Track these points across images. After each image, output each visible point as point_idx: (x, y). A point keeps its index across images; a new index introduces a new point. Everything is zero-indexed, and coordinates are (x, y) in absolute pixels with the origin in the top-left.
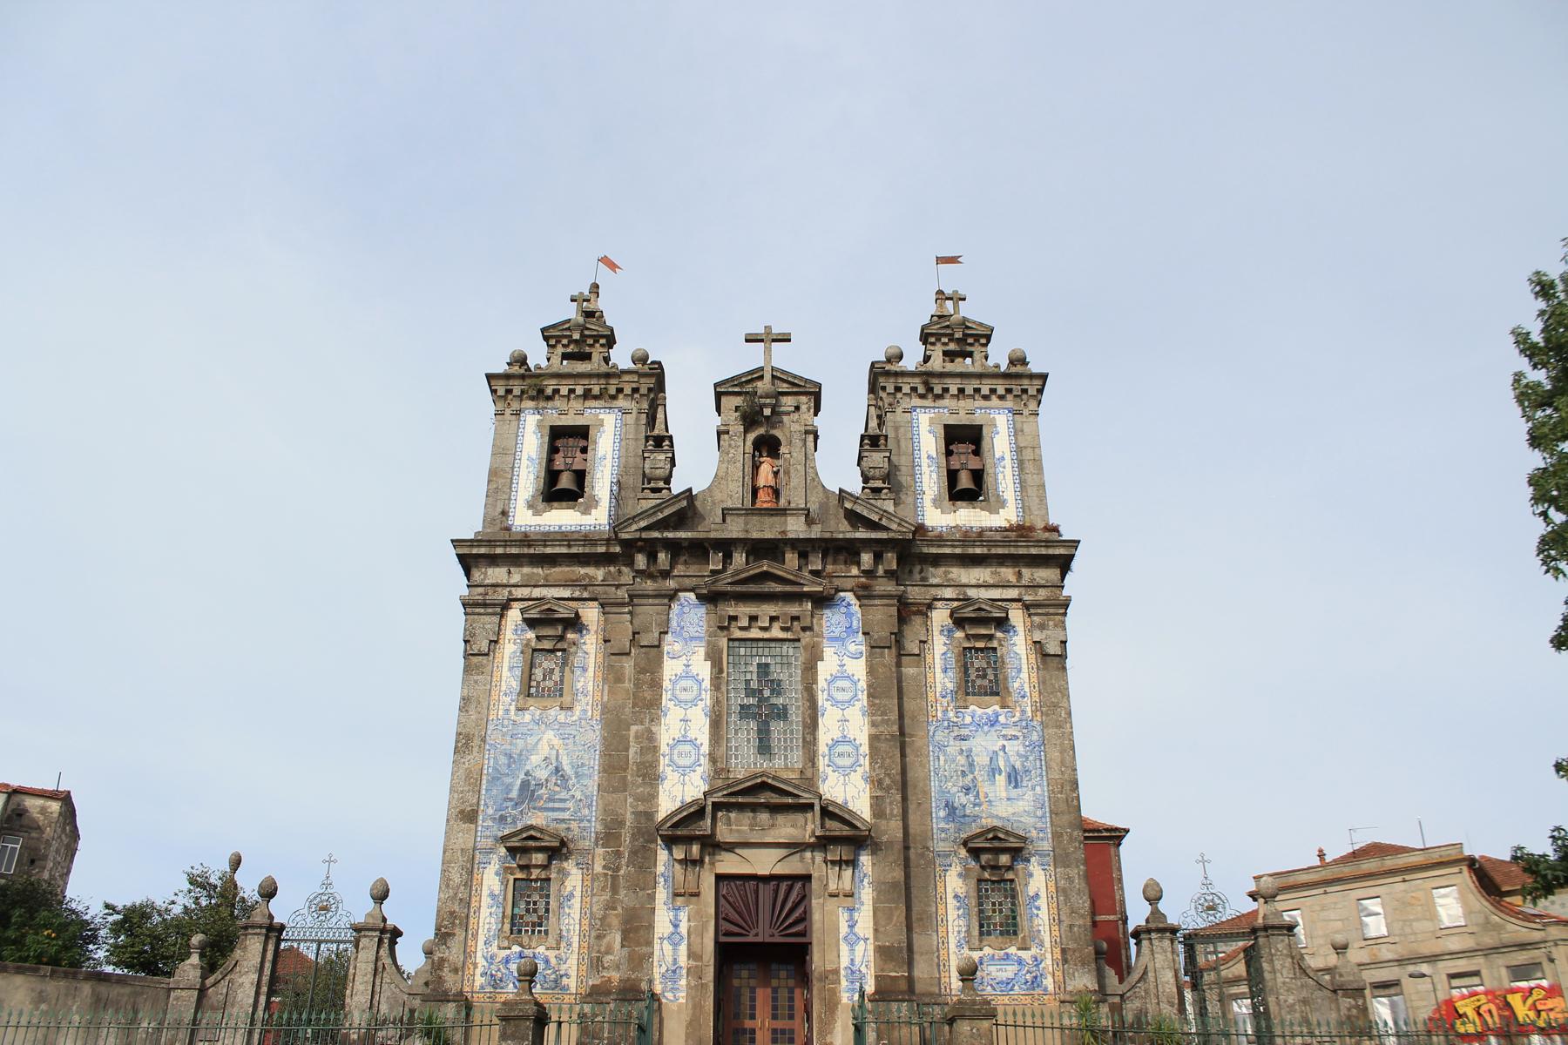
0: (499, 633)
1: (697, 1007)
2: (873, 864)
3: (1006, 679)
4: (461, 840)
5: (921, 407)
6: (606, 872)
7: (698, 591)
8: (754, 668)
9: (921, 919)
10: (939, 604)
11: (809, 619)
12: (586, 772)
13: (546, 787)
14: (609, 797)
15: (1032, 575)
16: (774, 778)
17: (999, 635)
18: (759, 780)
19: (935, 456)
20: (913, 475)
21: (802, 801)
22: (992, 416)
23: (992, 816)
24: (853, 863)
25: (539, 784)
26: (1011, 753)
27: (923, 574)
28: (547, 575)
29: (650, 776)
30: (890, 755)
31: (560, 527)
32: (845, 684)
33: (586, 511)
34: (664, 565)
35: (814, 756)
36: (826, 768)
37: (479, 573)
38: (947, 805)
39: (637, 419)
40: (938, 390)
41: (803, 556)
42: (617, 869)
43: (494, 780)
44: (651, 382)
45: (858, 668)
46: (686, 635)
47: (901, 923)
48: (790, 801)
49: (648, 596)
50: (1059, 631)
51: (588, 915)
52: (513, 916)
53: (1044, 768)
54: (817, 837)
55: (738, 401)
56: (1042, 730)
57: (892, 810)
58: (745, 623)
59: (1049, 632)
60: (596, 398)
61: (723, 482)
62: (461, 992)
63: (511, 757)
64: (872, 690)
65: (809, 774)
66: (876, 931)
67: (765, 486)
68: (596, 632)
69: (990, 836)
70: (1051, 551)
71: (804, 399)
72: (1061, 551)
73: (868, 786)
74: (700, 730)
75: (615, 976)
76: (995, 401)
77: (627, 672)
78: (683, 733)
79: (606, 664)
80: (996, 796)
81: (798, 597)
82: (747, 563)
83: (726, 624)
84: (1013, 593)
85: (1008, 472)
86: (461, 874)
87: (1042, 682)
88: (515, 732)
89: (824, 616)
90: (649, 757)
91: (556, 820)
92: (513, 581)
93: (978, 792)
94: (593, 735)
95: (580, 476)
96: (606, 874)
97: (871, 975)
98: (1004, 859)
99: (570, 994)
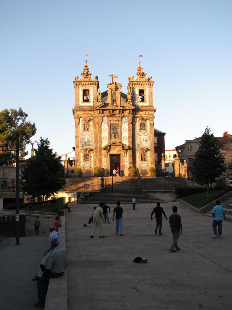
3: (146, 128)
14: (96, 144)
29: (101, 141)
32: (125, 129)
33: (89, 103)
40: (138, 84)
42: (97, 153)
44: (97, 83)
45: (127, 127)
55: (110, 87)
74: (107, 135)
75: (98, 166)
76: (146, 86)
82: (113, 112)
84: (147, 116)
90: (101, 139)
94: (93, 136)
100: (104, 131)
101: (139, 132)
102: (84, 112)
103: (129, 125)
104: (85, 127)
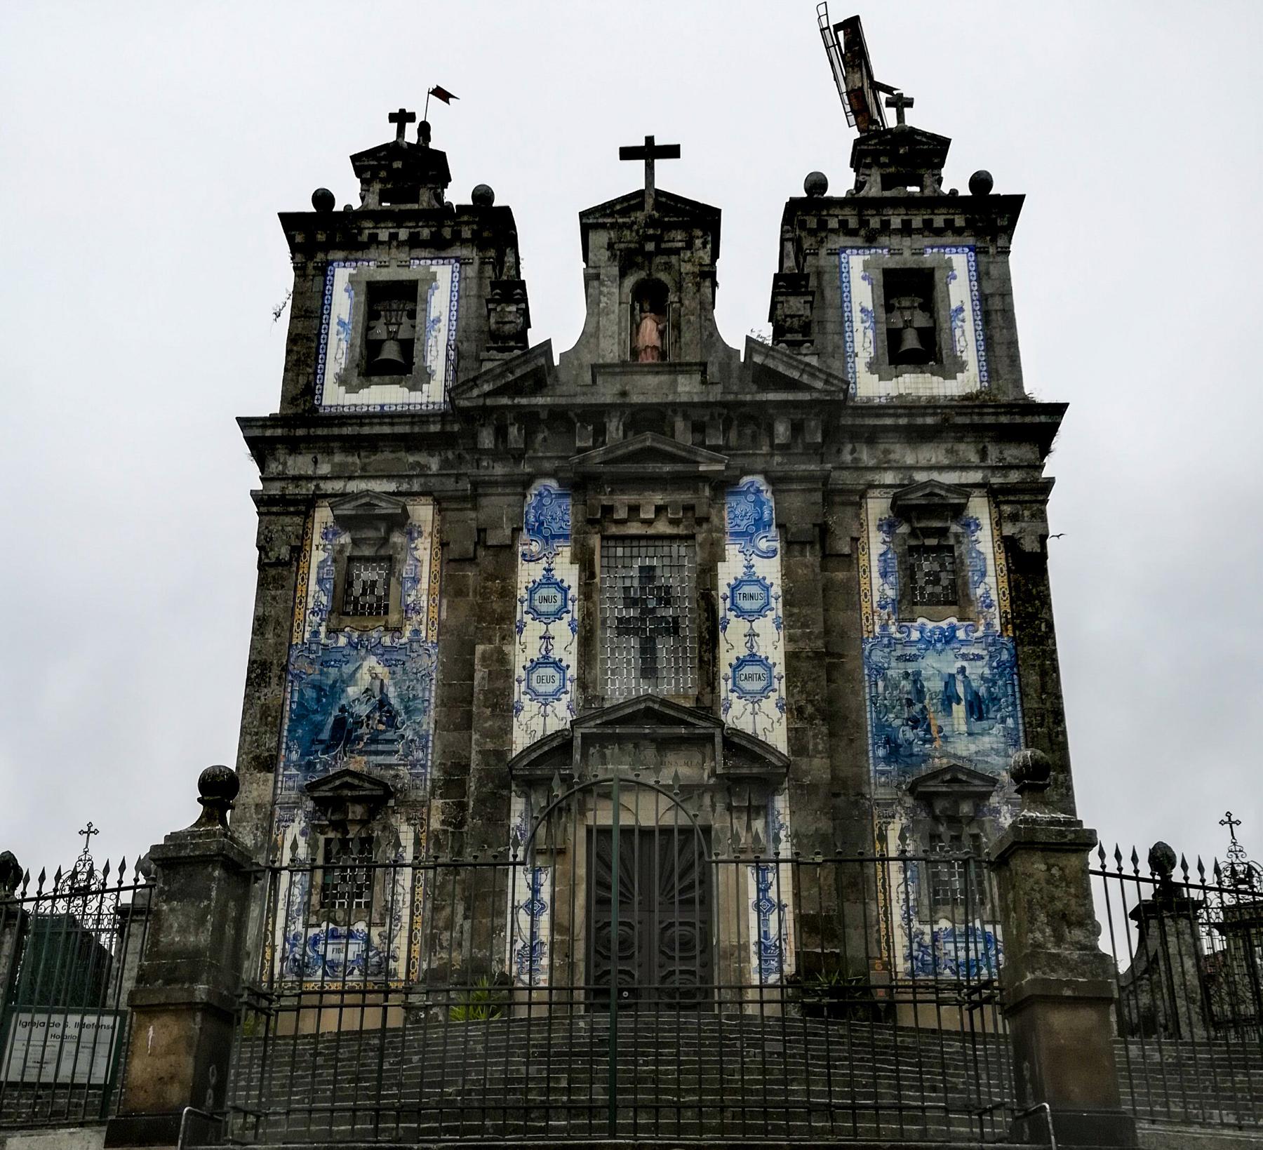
0: (303, 538)
2: (792, 813)
3: (966, 584)
4: (255, 794)
5: (852, 248)
6: (445, 828)
7: (561, 475)
8: (635, 573)
9: (855, 884)
10: (876, 492)
11: (705, 508)
12: (420, 706)
13: (368, 725)
14: (452, 736)
15: (1001, 453)
16: (664, 702)
17: (955, 528)
18: (642, 706)
19: (870, 308)
20: (842, 333)
21: (697, 731)
22: (947, 256)
24: (762, 809)
25: (358, 723)
26: (973, 677)
27: (855, 455)
28: (365, 464)
29: (504, 708)
30: (813, 676)
31: (382, 406)
33: (415, 387)
34: (516, 442)
35: (714, 679)
36: (730, 694)
37: (276, 464)
38: (888, 741)
39: (481, 272)
40: (875, 223)
41: (698, 428)
43: (302, 714)
45: (771, 570)
46: (546, 533)
47: (830, 886)
48: (683, 731)
49: (495, 484)
50: (1036, 524)
51: (422, 882)
52: (325, 887)
53: (1018, 695)
54: (718, 776)
56: (1015, 648)
57: (816, 745)
58: (622, 514)
59: (1023, 525)
60: (424, 245)
61: (592, 340)
64: (789, 597)
65: (707, 701)
66: (797, 895)
67: (647, 347)
68: (431, 534)
69: (948, 777)
73: (784, 715)
76: (949, 239)
77: (471, 582)
78: (544, 653)
79: (444, 574)
80: (953, 731)
81: (692, 480)
83: (599, 516)
84: (975, 477)
85: (969, 326)
86: (255, 835)
87: (1014, 587)
88: (326, 658)
89: (726, 506)
90: (499, 684)
91: (380, 765)
93: (929, 725)
95: (407, 347)
96: (445, 832)
97: (791, 952)
98: (966, 808)
99: (397, 981)
100: (538, 615)
101: (893, 629)
104: (357, 589)
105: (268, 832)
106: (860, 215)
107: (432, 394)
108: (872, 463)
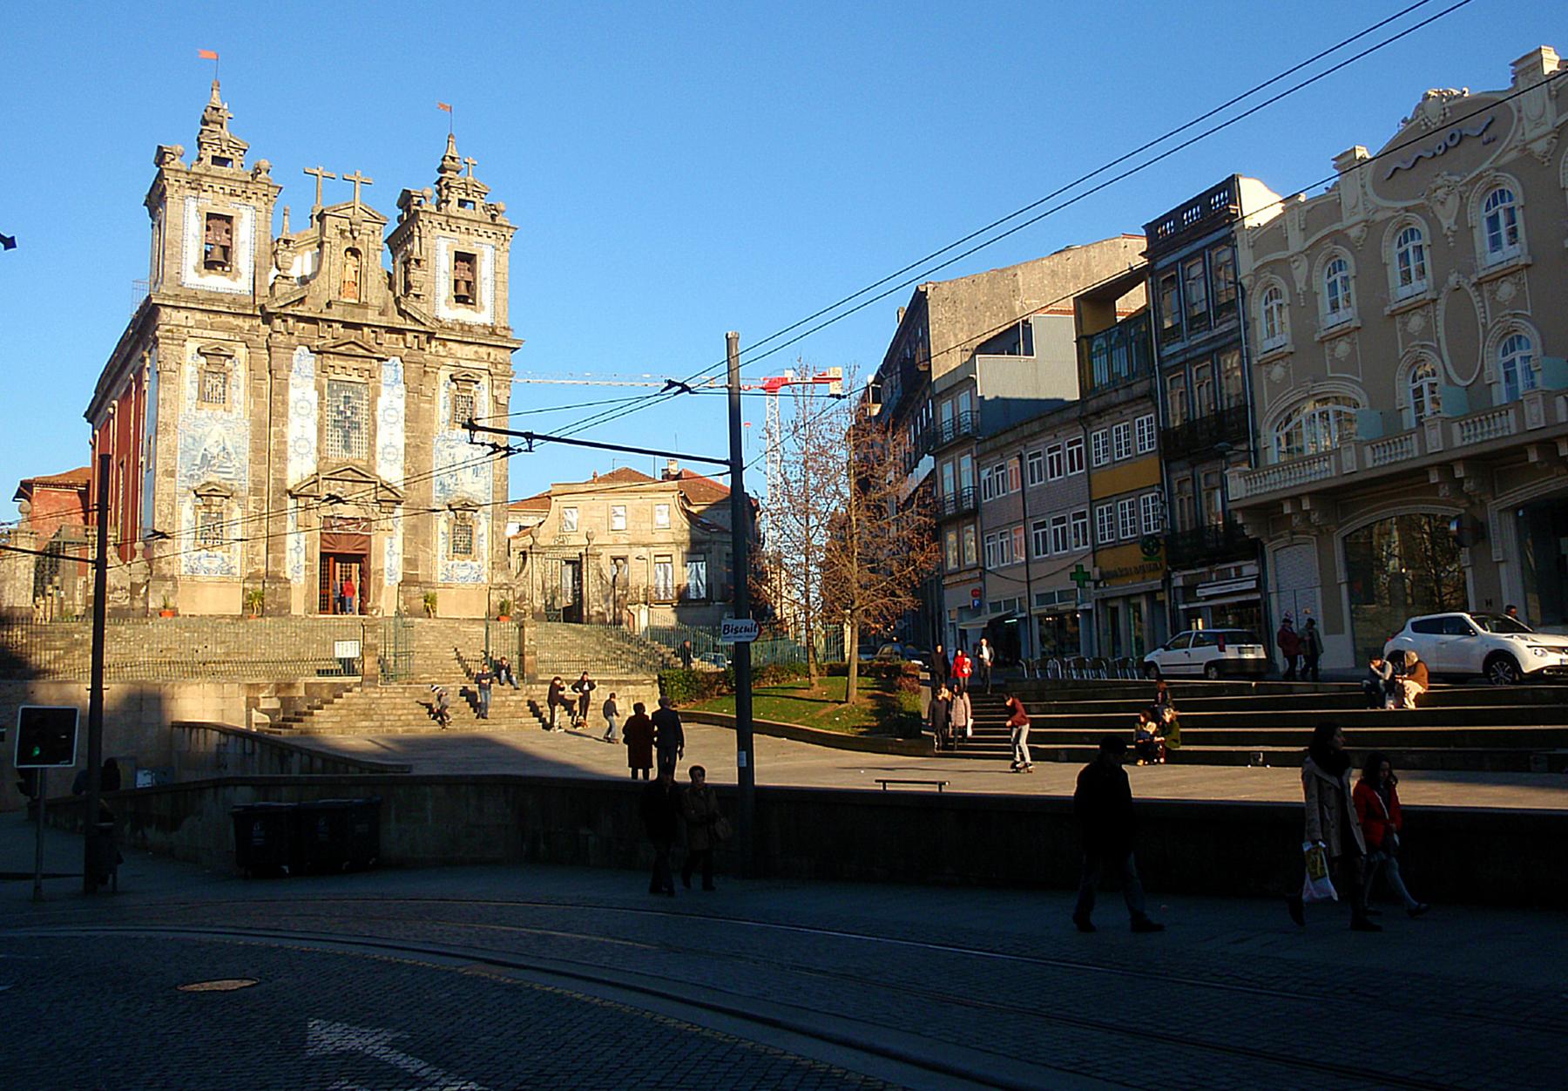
1: (311, 586)
17: (474, 387)
23: (463, 491)
32: (393, 412)
50: (507, 390)
62: (172, 576)
63: (195, 439)
70: (508, 345)
71: (377, 226)
72: (515, 346)
74: (312, 433)
76: (485, 239)
84: (485, 366)
90: (282, 447)
92: (189, 325)
102: (204, 317)
103: (408, 397)
105: (173, 508)
106: (447, 221)
107: (242, 285)
108: (444, 354)
